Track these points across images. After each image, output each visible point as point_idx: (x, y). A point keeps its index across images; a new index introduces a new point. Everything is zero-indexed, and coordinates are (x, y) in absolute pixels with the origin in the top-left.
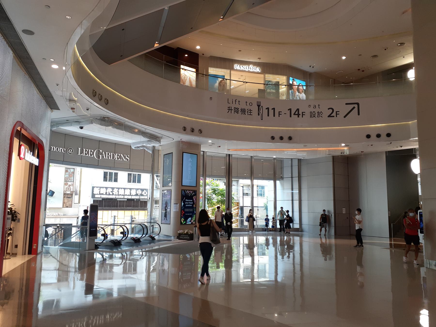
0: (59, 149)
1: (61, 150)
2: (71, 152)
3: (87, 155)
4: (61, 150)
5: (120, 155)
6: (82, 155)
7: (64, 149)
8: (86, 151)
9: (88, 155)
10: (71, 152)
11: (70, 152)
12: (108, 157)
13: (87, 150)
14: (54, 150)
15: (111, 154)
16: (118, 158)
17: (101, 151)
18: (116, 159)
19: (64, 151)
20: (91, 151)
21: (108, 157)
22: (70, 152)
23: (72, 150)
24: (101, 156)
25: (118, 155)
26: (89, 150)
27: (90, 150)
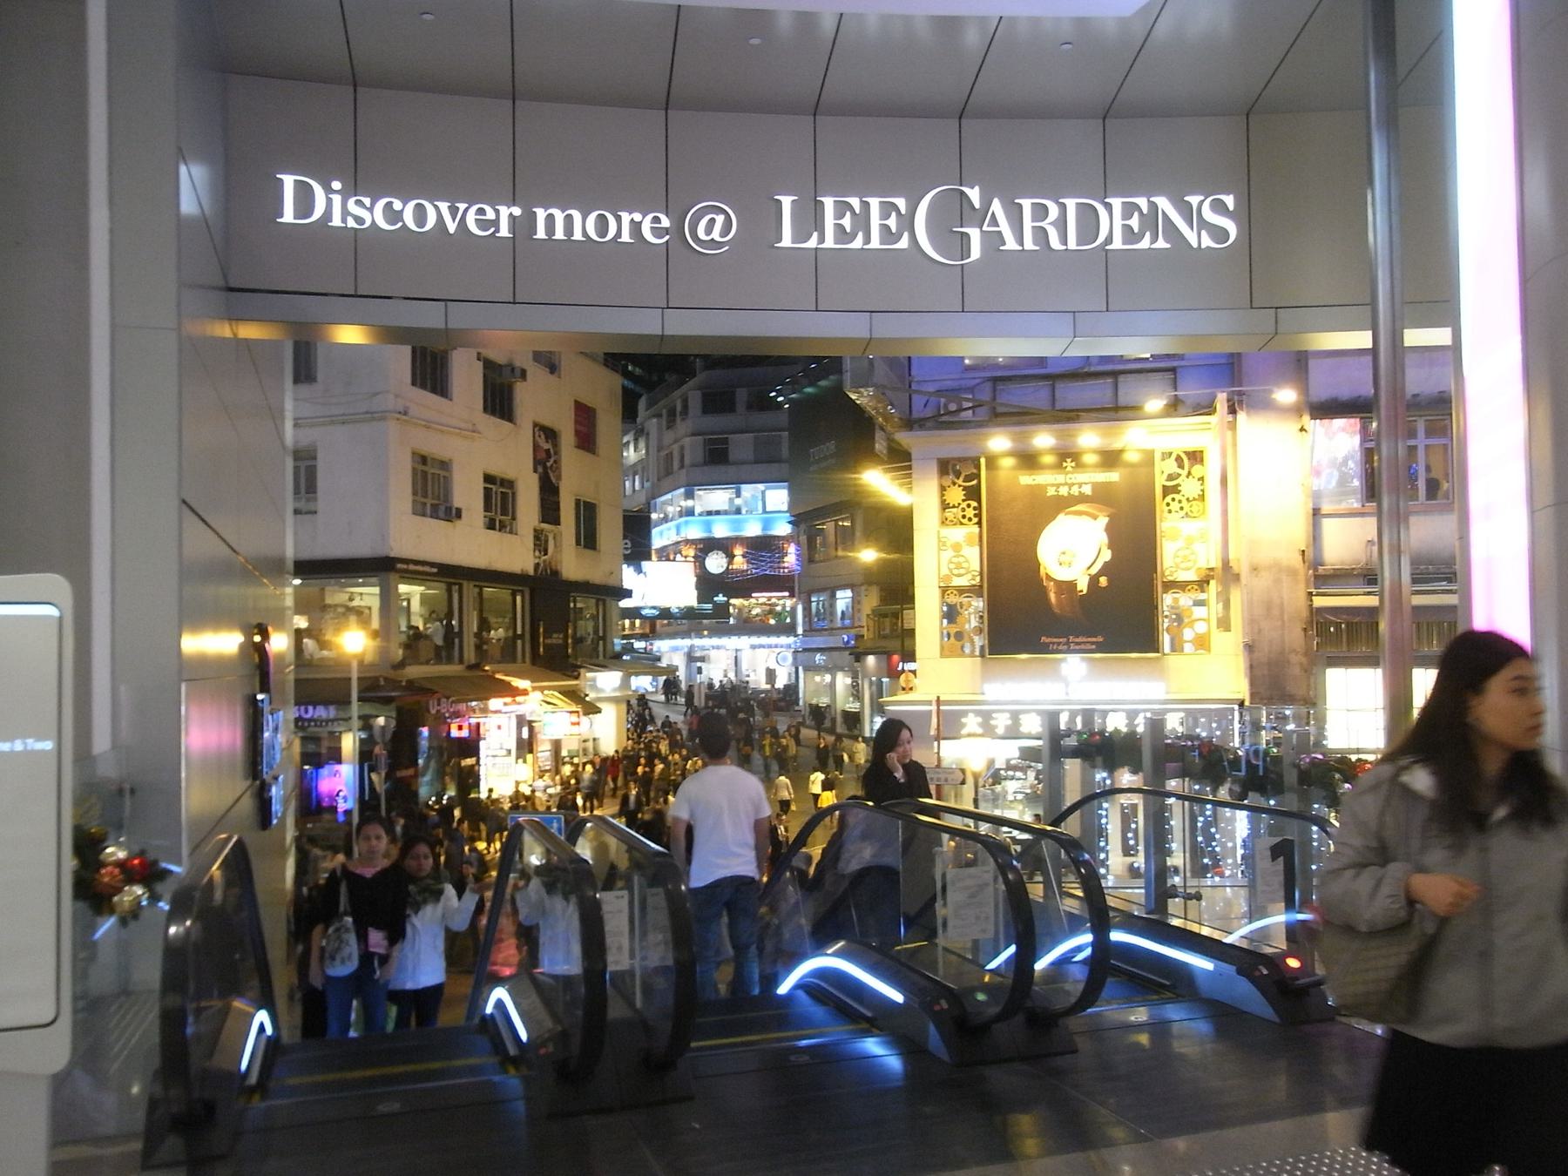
0: (619, 219)
1: (636, 227)
2: (716, 235)
3: (858, 243)
4: (636, 227)
5: (1154, 207)
6: (812, 243)
7: (656, 220)
8: (842, 209)
9: (867, 240)
10: (716, 235)
11: (709, 230)
12: (1041, 235)
13: (855, 202)
14: (578, 236)
15: (1063, 207)
16: (1130, 235)
17: (974, 194)
18: (1117, 244)
19: (657, 232)
20: (889, 208)
21: (1041, 235)
22: (709, 230)
23: (720, 219)
24: (974, 234)
25: (1129, 210)
26: (866, 206)
27: (874, 203)
